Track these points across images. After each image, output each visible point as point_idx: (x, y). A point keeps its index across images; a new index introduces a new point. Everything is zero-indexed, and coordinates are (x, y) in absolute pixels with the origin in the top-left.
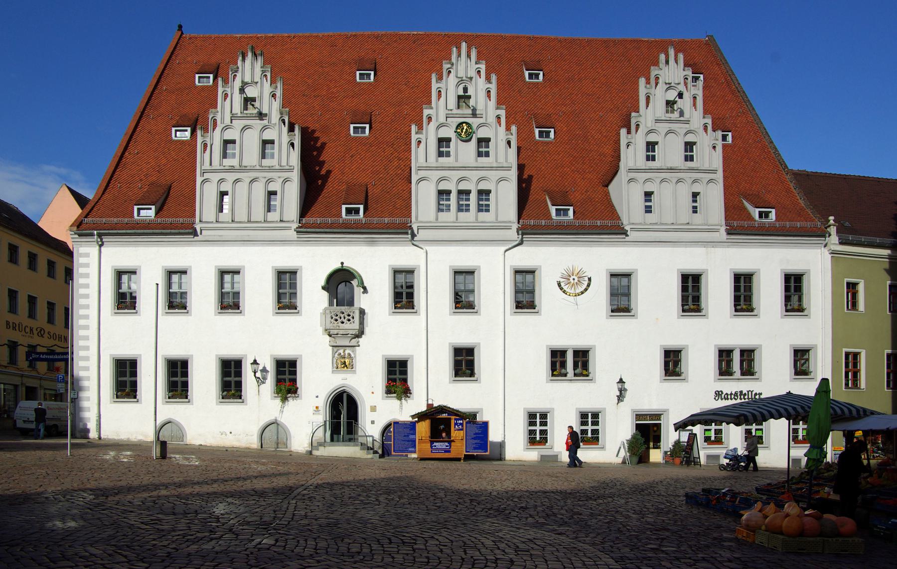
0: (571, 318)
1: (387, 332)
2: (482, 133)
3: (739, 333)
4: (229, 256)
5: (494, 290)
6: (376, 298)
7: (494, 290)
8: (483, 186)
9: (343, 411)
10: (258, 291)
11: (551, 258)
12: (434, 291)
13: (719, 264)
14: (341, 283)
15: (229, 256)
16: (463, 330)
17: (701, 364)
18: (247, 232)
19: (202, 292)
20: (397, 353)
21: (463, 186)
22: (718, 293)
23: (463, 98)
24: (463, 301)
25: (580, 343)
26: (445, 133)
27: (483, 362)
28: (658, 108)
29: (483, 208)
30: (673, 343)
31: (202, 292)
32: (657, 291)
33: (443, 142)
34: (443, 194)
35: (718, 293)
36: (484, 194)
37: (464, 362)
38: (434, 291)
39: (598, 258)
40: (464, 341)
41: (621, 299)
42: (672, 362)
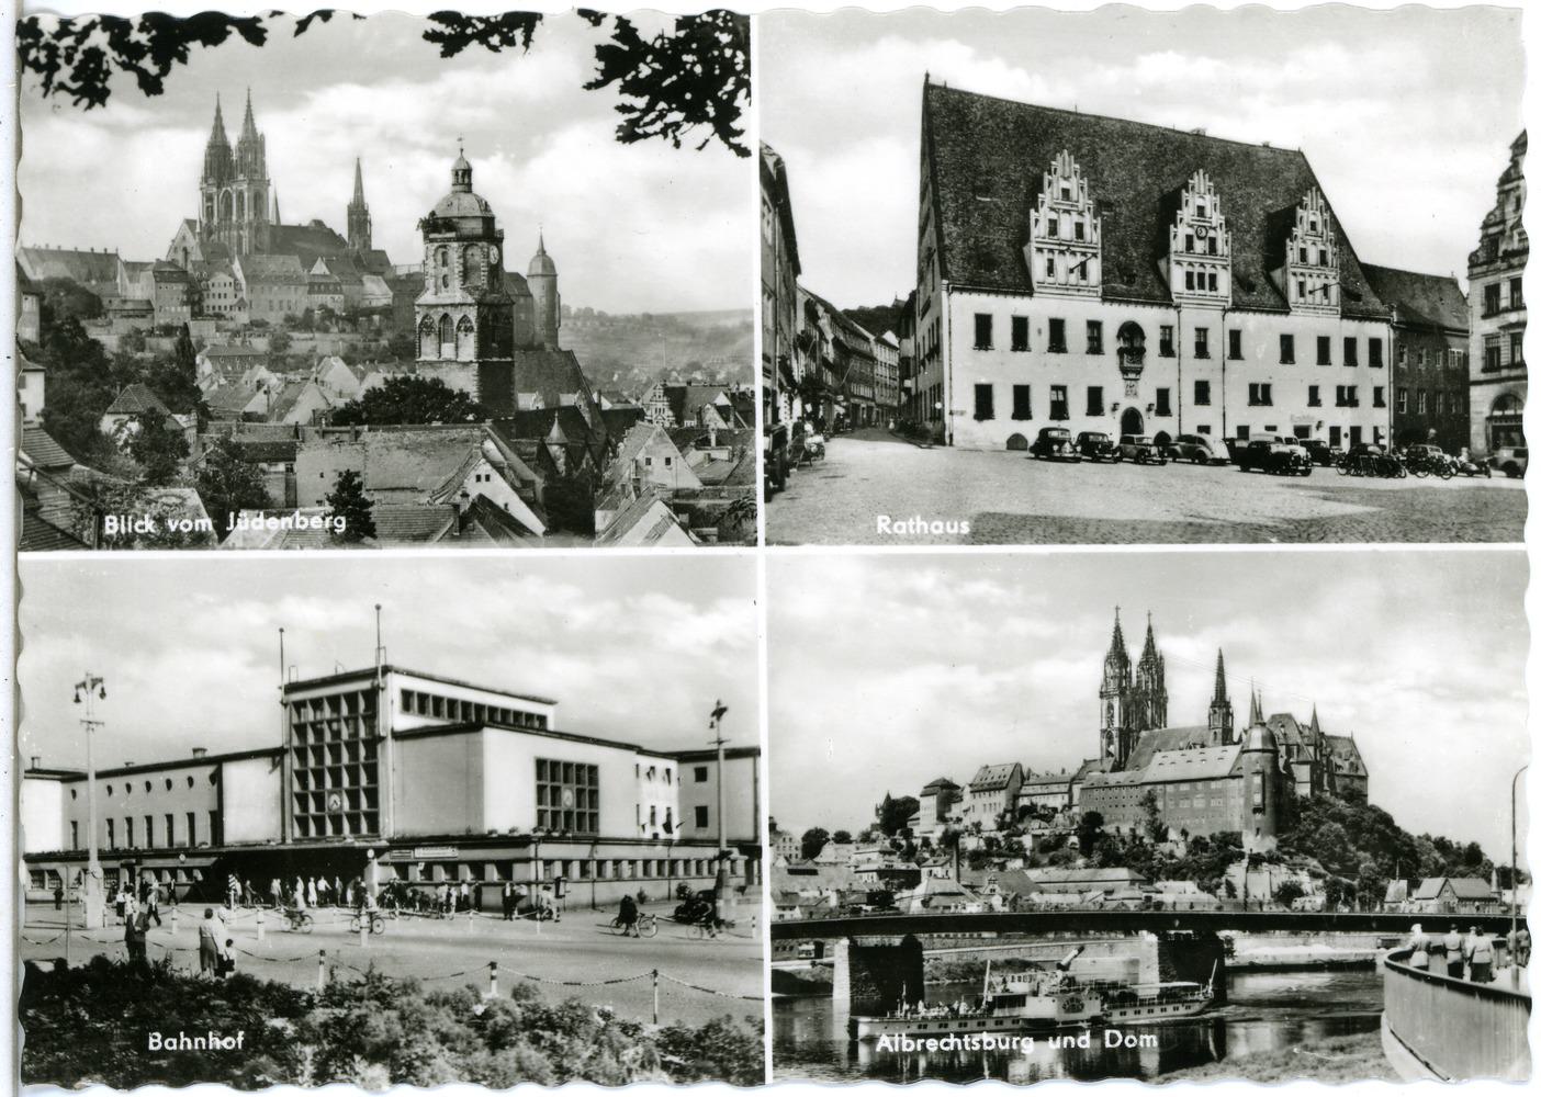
2: (1212, 234)
3: (1347, 376)
5: (1218, 344)
7: (1218, 344)
8: (1213, 271)
9: (1131, 421)
10: (1076, 336)
12: (1186, 342)
13: (1339, 329)
17: (1328, 396)
20: (1163, 385)
21: (1201, 270)
22: (1337, 352)
23: (1201, 210)
24: (1202, 350)
26: (1190, 231)
27: (1215, 393)
28: (1307, 227)
29: (1213, 286)
32: (1306, 351)
33: (1189, 239)
34: (1189, 275)
35: (1337, 352)
36: (1213, 277)
37: (1202, 393)
38: (1186, 342)
39: (1280, 324)
41: (1287, 355)
42: (1314, 391)
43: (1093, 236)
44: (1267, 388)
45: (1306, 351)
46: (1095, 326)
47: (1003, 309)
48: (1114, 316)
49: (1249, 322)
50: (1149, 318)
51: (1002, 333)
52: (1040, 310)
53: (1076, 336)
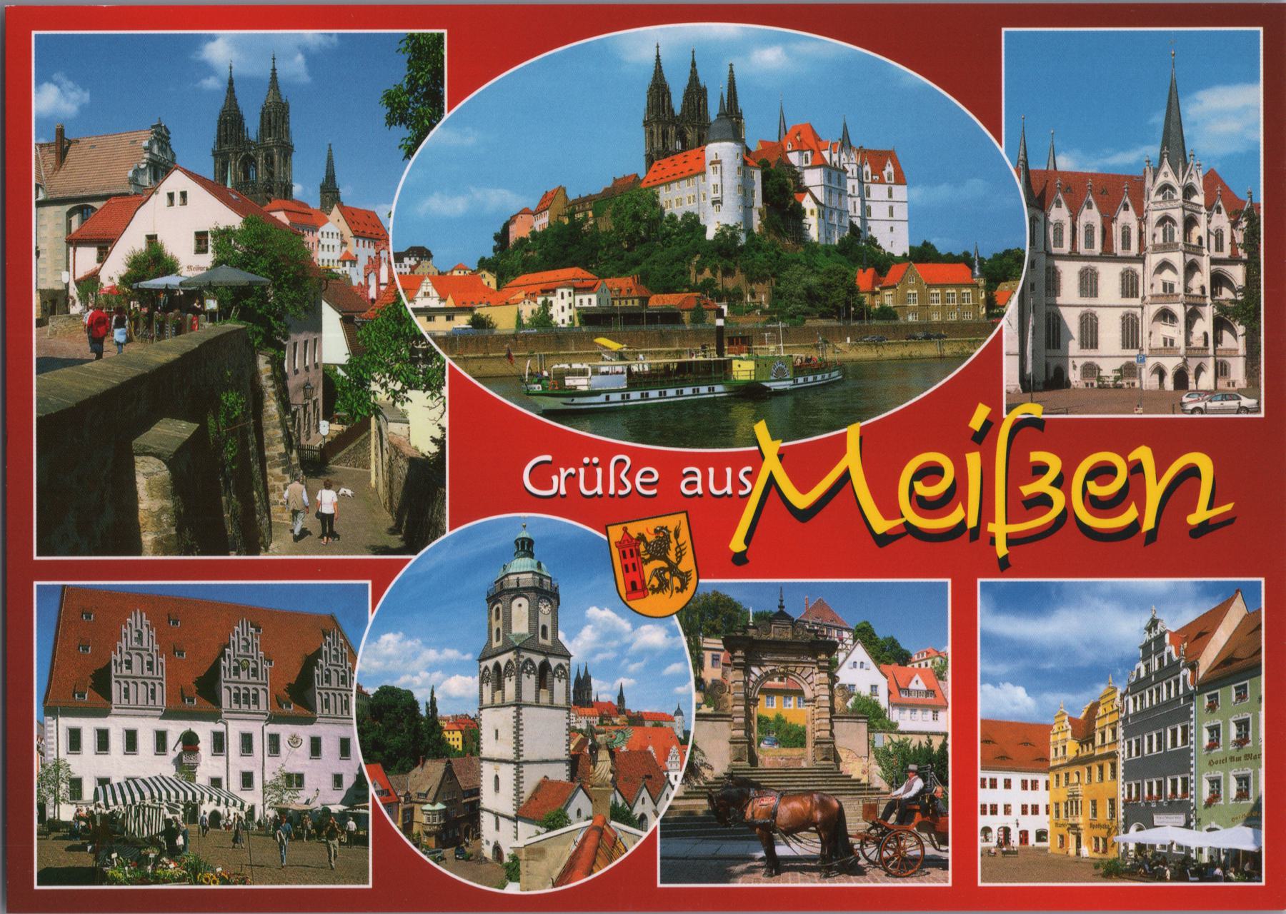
0: (295, 759)
1: (208, 765)
4: (131, 723)
6: (205, 745)
10: (146, 742)
11: (285, 731)
12: (234, 743)
14: (190, 741)
15: (131, 723)
16: (247, 764)
18: (141, 711)
19: (117, 742)
25: (299, 770)
30: (338, 771)
31: (117, 742)
32: (330, 747)
34: (237, 696)
36: (256, 697)
38: (234, 743)
40: (247, 769)
43: (160, 672)
44: (300, 777)
45: (330, 747)
46: (161, 738)
47: (88, 727)
48: (175, 729)
49: (285, 731)
50: (204, 730)
51: (88, 740)
52: (116, 726)
53: (146, 742)
